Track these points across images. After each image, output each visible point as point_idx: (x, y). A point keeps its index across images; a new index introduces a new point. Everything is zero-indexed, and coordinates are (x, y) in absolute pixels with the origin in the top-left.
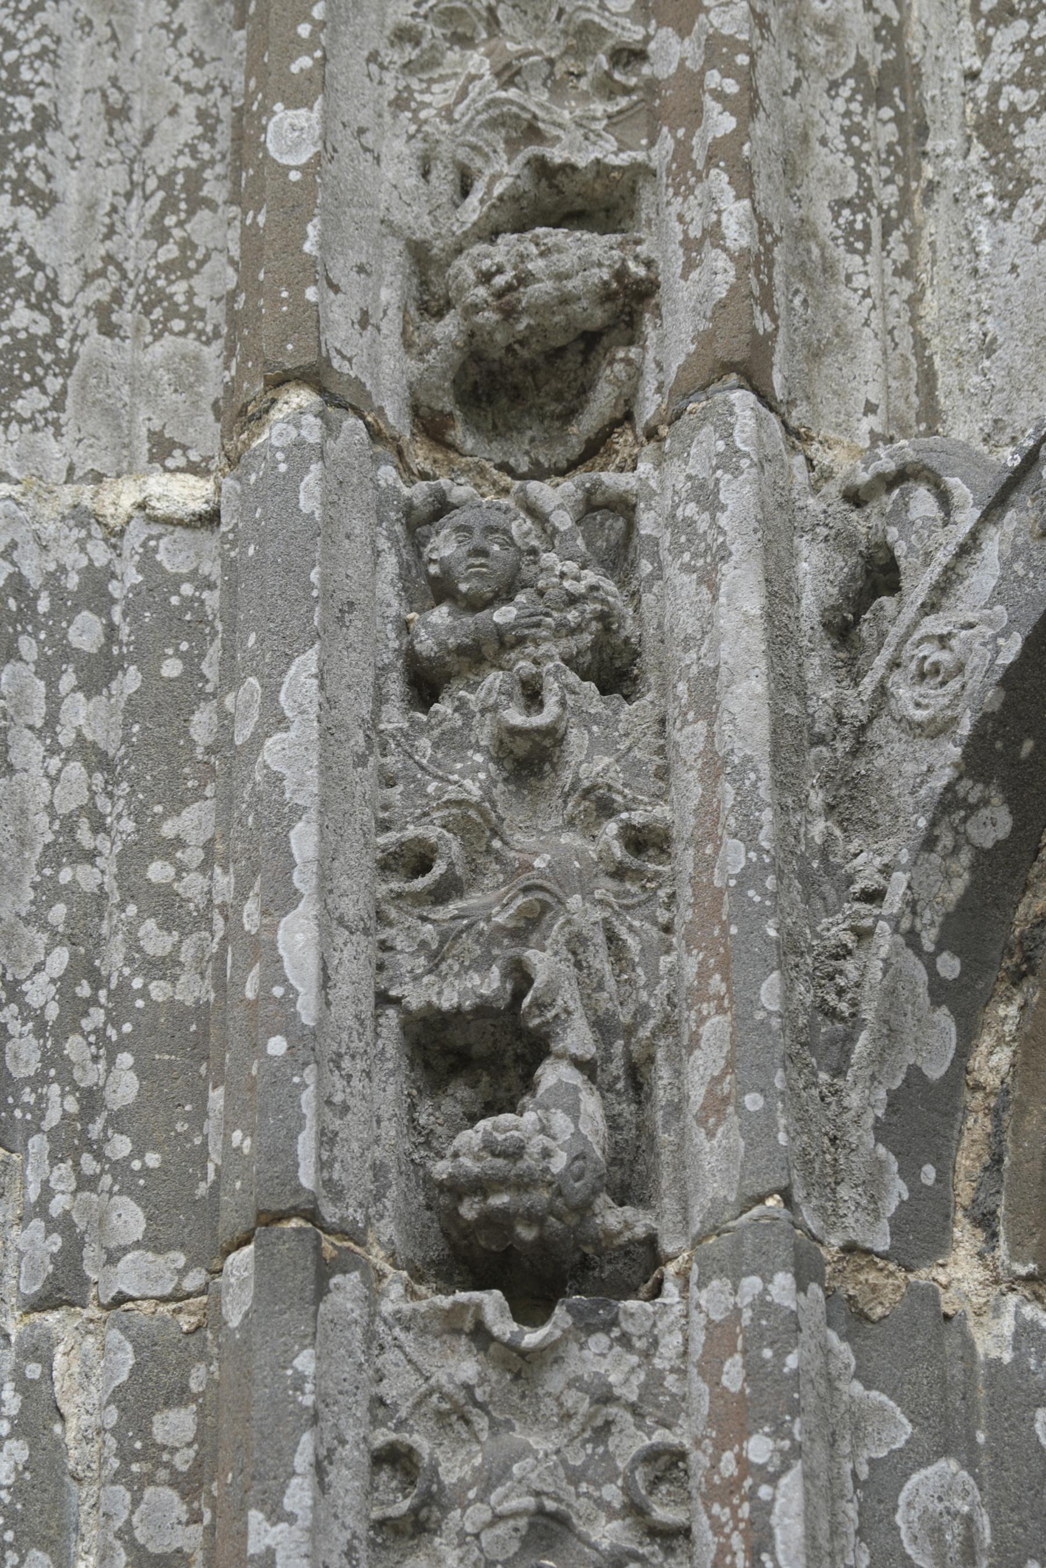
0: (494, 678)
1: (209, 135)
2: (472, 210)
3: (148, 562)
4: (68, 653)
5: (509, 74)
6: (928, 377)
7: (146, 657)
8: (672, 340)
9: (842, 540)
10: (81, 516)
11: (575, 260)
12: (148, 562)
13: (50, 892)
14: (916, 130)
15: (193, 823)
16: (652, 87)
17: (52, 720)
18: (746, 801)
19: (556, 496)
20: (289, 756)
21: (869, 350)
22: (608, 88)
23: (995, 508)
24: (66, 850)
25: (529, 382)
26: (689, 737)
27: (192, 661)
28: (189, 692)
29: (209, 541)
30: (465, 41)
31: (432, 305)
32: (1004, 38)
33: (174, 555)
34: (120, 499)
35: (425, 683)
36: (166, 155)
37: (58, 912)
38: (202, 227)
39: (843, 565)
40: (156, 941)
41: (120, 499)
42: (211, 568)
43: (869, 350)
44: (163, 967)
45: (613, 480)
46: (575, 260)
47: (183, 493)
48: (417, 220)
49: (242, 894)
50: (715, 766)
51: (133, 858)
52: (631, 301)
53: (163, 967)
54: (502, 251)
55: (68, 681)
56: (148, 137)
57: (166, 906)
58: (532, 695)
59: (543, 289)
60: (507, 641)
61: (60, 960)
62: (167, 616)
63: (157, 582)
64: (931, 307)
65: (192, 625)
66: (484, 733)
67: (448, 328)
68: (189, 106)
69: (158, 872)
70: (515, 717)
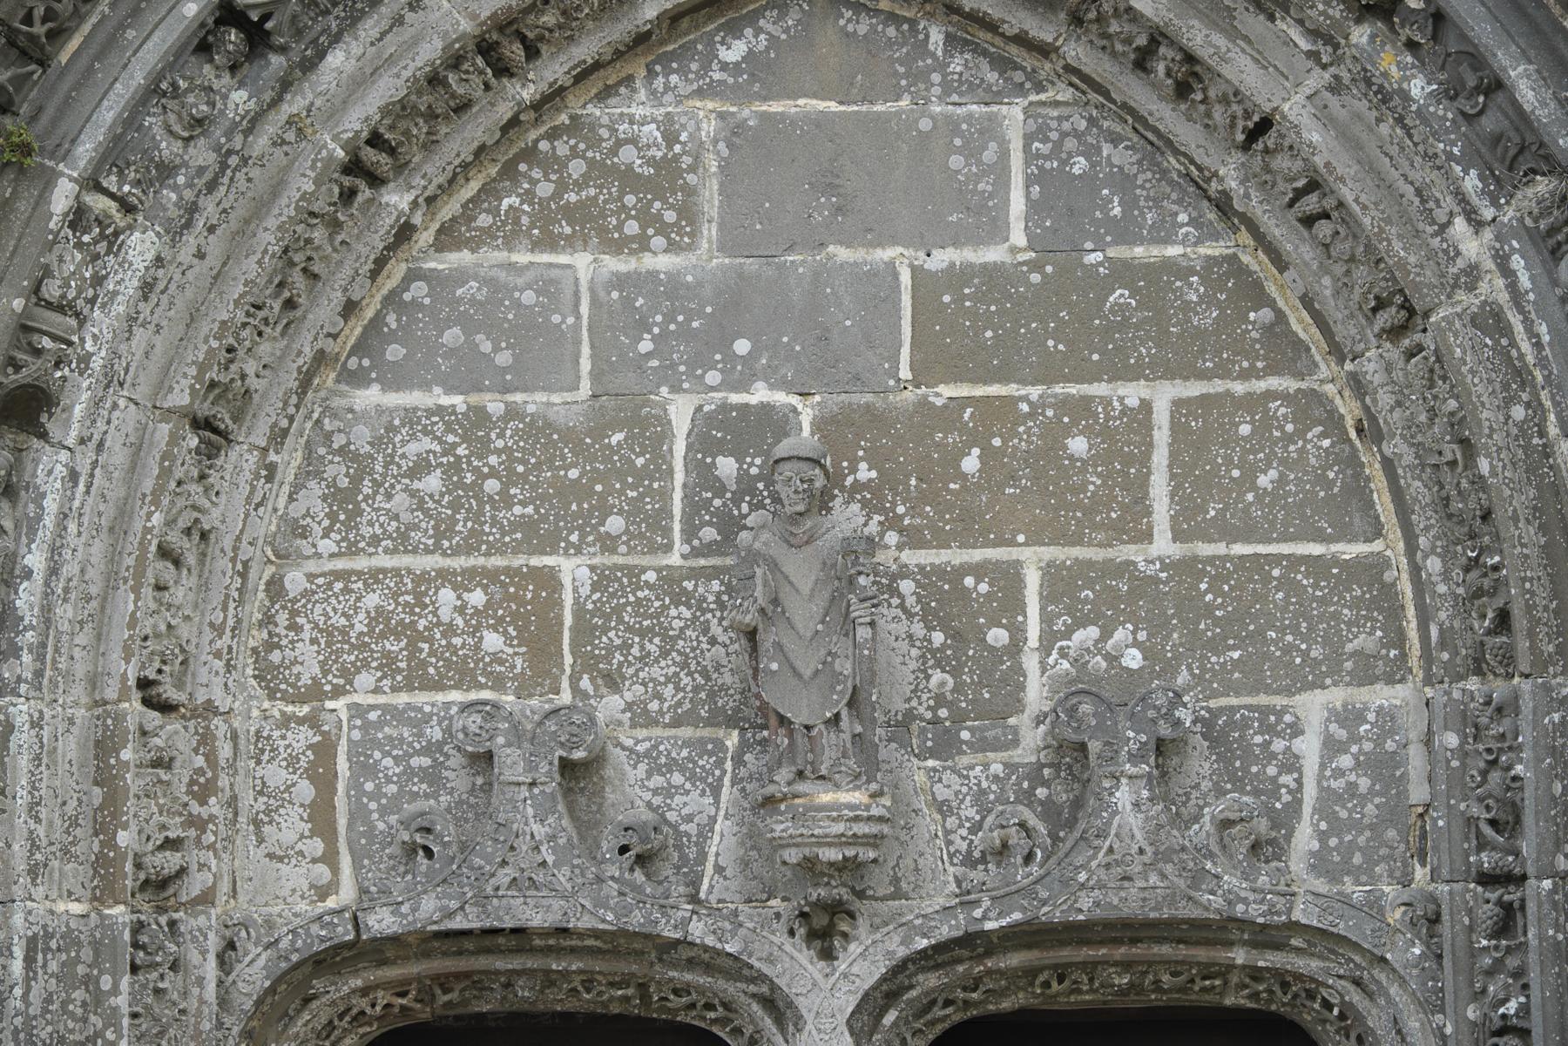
0: (155, 974)
1: (80, 805)
2: (150, 846)
3: (67, 926)
4: (50, 949)
5: (161, 813)
6: (235, 882)
7: (68, 952)
8: (196, 884)
9: (224, 938)
10: (52, 912)
11: (172, 861)
12: (67, 926)
13: (45, 1011)
14: (236, 814)
15: (79, 995)
16: (190, 814)
17: (45, 966)
18: (210, 1013)
19: (163, 920)
20: (122, 1001)
21: (226, 878)
22: (181, 814)
23: (266, 949)
24: (48, 1000)
25: (159, 886)
26: (196, 991)
27: (78, 952)
28: (77, 960)
29: (82, 921)
30: (148, 796)
31: (138, 866)
32: (262, 799)
33: (73, 925)
34: (61, 907)
35: (135, 969)
36: (70, 809)
37: (49, 1016)
38: (78, 831)
39: (224, 944)
40: (71, 1024)
41: (61, 907)
42: (83, 929)
43: (226, 878)
44: (72, 1031)
45: (176, 916)
46: (172, 861)
47: (77, 908)
48: (137, 847)
49: (106, 1027)
50: (202, 1001)
51: (64, 1004)
52: (182, 871)
53: (72, 1031)
54: (159, 859)
55: (49, 956)
56: (64, 803)
57: (72, 1015)
58: (162, 977)
59: (166, 871)
60: (158, 964)
61: (49, 1029)
62: (71, 940)
63: (70, 931)
64: (237, 862)
65: (79, 944)
66: (151, 986)
67: (142, 876)
68: (75, 796)
69: (71, 1007)
70: (161, 985)
